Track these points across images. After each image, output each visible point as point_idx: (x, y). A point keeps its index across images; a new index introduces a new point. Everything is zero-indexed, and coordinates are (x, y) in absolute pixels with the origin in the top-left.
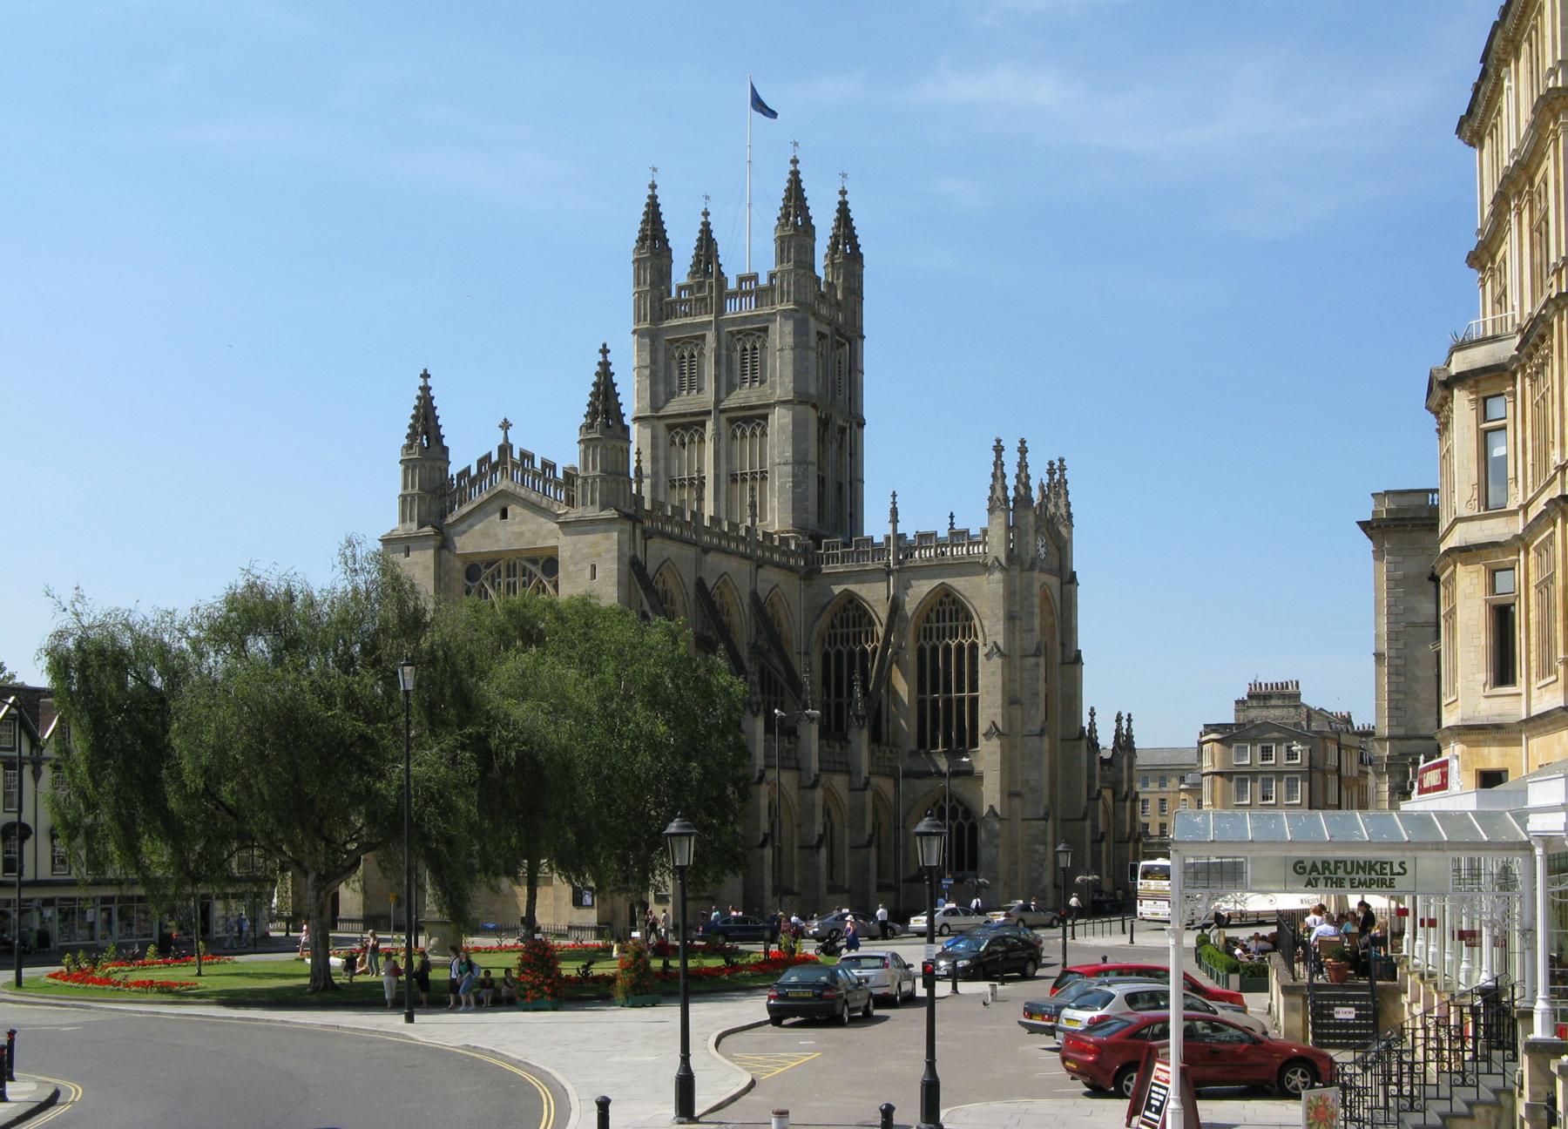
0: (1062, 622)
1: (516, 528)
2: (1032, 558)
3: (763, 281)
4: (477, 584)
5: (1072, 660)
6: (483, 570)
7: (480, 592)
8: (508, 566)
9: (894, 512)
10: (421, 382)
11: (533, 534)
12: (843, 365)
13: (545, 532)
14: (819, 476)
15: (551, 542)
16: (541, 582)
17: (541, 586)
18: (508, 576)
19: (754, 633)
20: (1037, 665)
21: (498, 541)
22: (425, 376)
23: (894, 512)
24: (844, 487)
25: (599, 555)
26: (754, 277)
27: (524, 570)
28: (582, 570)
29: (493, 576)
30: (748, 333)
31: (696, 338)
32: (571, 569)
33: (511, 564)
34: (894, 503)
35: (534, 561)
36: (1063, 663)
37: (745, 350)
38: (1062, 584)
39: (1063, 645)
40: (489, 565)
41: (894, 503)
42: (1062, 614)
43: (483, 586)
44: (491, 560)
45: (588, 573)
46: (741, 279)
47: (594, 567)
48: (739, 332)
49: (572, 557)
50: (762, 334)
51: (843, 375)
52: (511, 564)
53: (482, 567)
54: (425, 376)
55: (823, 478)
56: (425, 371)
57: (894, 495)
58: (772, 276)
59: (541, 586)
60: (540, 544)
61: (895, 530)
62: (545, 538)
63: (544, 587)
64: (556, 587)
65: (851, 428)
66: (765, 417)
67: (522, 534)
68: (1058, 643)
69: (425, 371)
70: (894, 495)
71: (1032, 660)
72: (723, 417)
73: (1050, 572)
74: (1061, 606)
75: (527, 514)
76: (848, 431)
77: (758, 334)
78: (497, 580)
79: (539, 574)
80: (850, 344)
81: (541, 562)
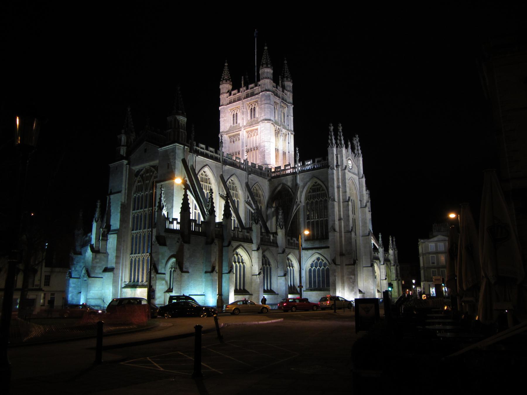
0: (360, 192)
2: (345, 166)
5: (364, 206)
12: (285, 114)
14: (276, 149)
19: (247, 197)
20: (348, 205)
24: (286, 153)
36: (361, 208)
38: (359, 179)
39: (361, 201)
42: (360, 189)
51: (285, 116)
55: (278, 150)
65: (288, 134)
66: (257, 129)
68: (358, 200)
71: (347, 203)
72: (245, 131)
73: (354, 174)
74: (359, 187)
76: (288, 135)
80: (288, 107)
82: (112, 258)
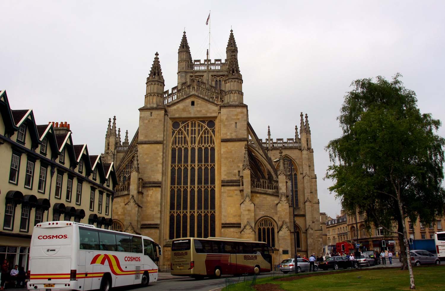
1: (199, 109)
3: (223, 61)
4: (178, 129)
6: (181, 124)
7: (179, 132)
8: (192, 123)
9: (269, 132)
10: (155, 56)
11: (206, 111)
13: (211, 111)
15: (214, 115)
16: (206, 129)
17: (206, 131)
18: (192, 127)
21: (190, 113)
22: (157, 54)
23: (269, 132)
25: (239, 119)
26: (220, 60)
27: (199, 125)
28: (231, 124)
29: (185, 127)
30: (218, 76)
31: (200, 76)
32: (226, 123)
33: (193, 122)
34: (269, 129)
35: (204, 122)
37: (217, 81)
40: (183, 123)
41: (269, 129)
43: (180, 130)
44: (185, 120)
45: (234, 125)
46: (216, 60)
47: (236, 123)
48: (215, 75)
49: (226, 119)
50: (223, 77)
52: (193, 122)
53: (180, 123)
54: (157, 54)
56: (157, 53)
57: (269, 127)
58: (226, 60)
59: (206, 131)
60: (209, 115)
61: (269, 137)
62: (211, 113)
63: (208, 132)
64: (213, 131)
67: (201, 111)
69: (157, 53)
70: (269, 127)
75: (204, 103)
77: (221, 77)
78: (187, 128)
79: (206, 127)
81: (207, 122)
82: (154, 213)
